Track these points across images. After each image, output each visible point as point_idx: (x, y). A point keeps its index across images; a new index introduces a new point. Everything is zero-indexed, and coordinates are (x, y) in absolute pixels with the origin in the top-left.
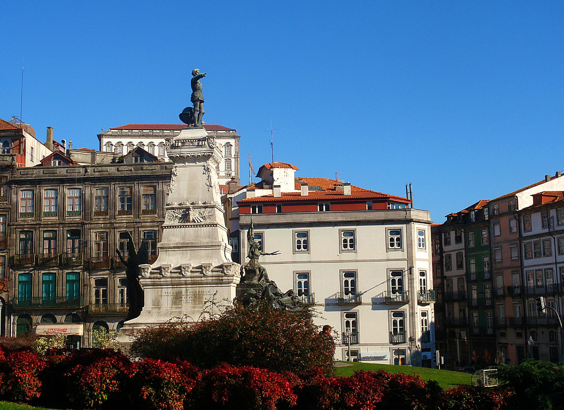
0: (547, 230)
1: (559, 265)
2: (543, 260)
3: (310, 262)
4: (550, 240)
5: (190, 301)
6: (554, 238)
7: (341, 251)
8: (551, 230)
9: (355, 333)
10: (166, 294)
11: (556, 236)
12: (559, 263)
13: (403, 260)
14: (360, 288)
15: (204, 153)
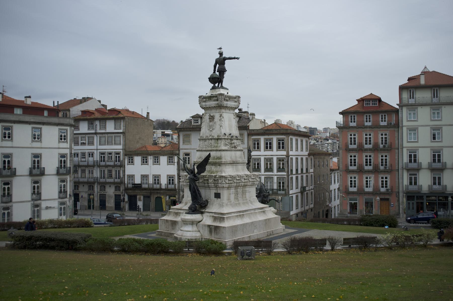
0: (93, 131)
1: (98, 151)
2: (87, 147)
3: (12, 147)
4: (93, 138)
5: (241, 197)
6: (97, 136)
7: (33, 141)
8: (96, 132)
9: (39, 194)
10: (232, 193)
11: (98, 136)
12: (99, 149)
13: (67, 148)
14: (43, 165)
15: (236, 106)
